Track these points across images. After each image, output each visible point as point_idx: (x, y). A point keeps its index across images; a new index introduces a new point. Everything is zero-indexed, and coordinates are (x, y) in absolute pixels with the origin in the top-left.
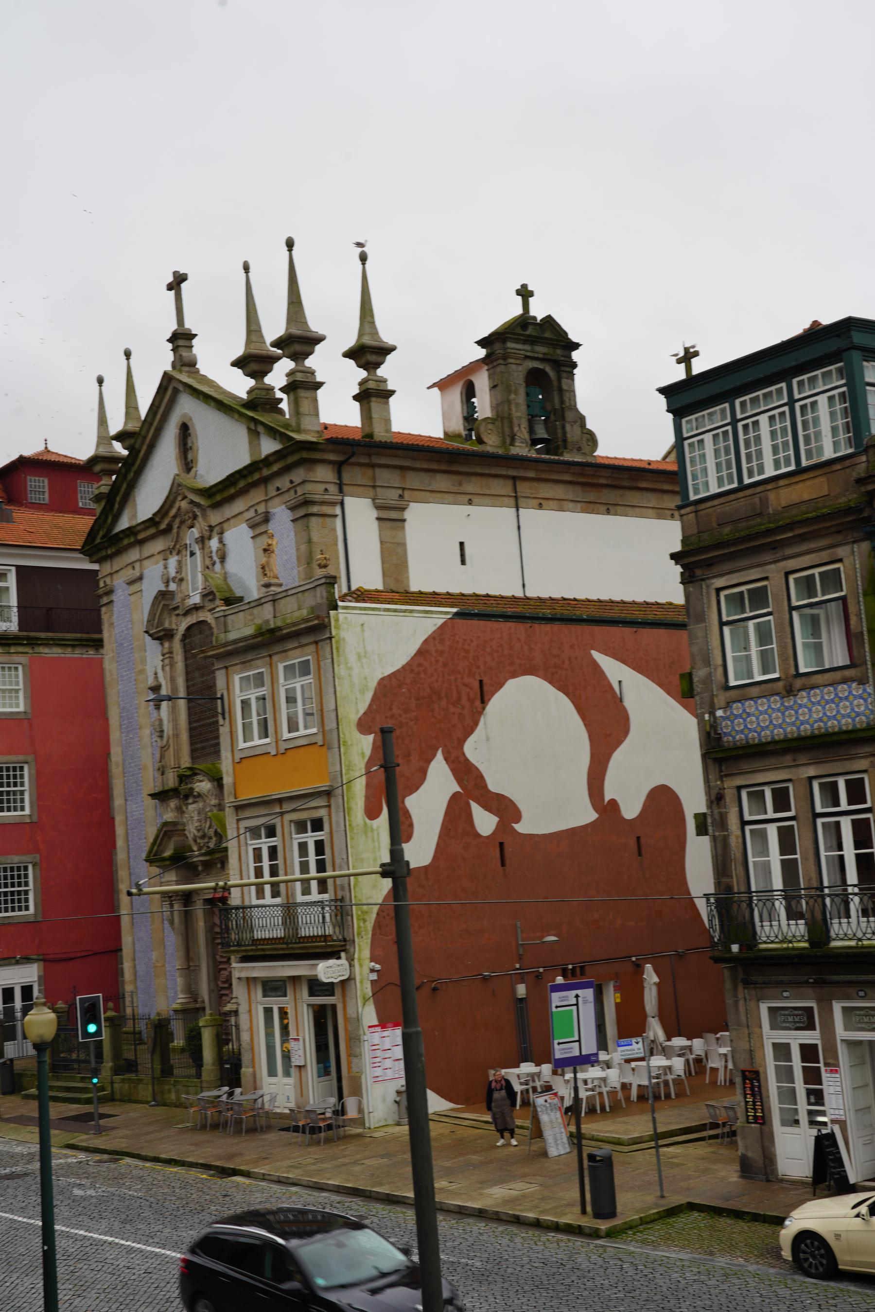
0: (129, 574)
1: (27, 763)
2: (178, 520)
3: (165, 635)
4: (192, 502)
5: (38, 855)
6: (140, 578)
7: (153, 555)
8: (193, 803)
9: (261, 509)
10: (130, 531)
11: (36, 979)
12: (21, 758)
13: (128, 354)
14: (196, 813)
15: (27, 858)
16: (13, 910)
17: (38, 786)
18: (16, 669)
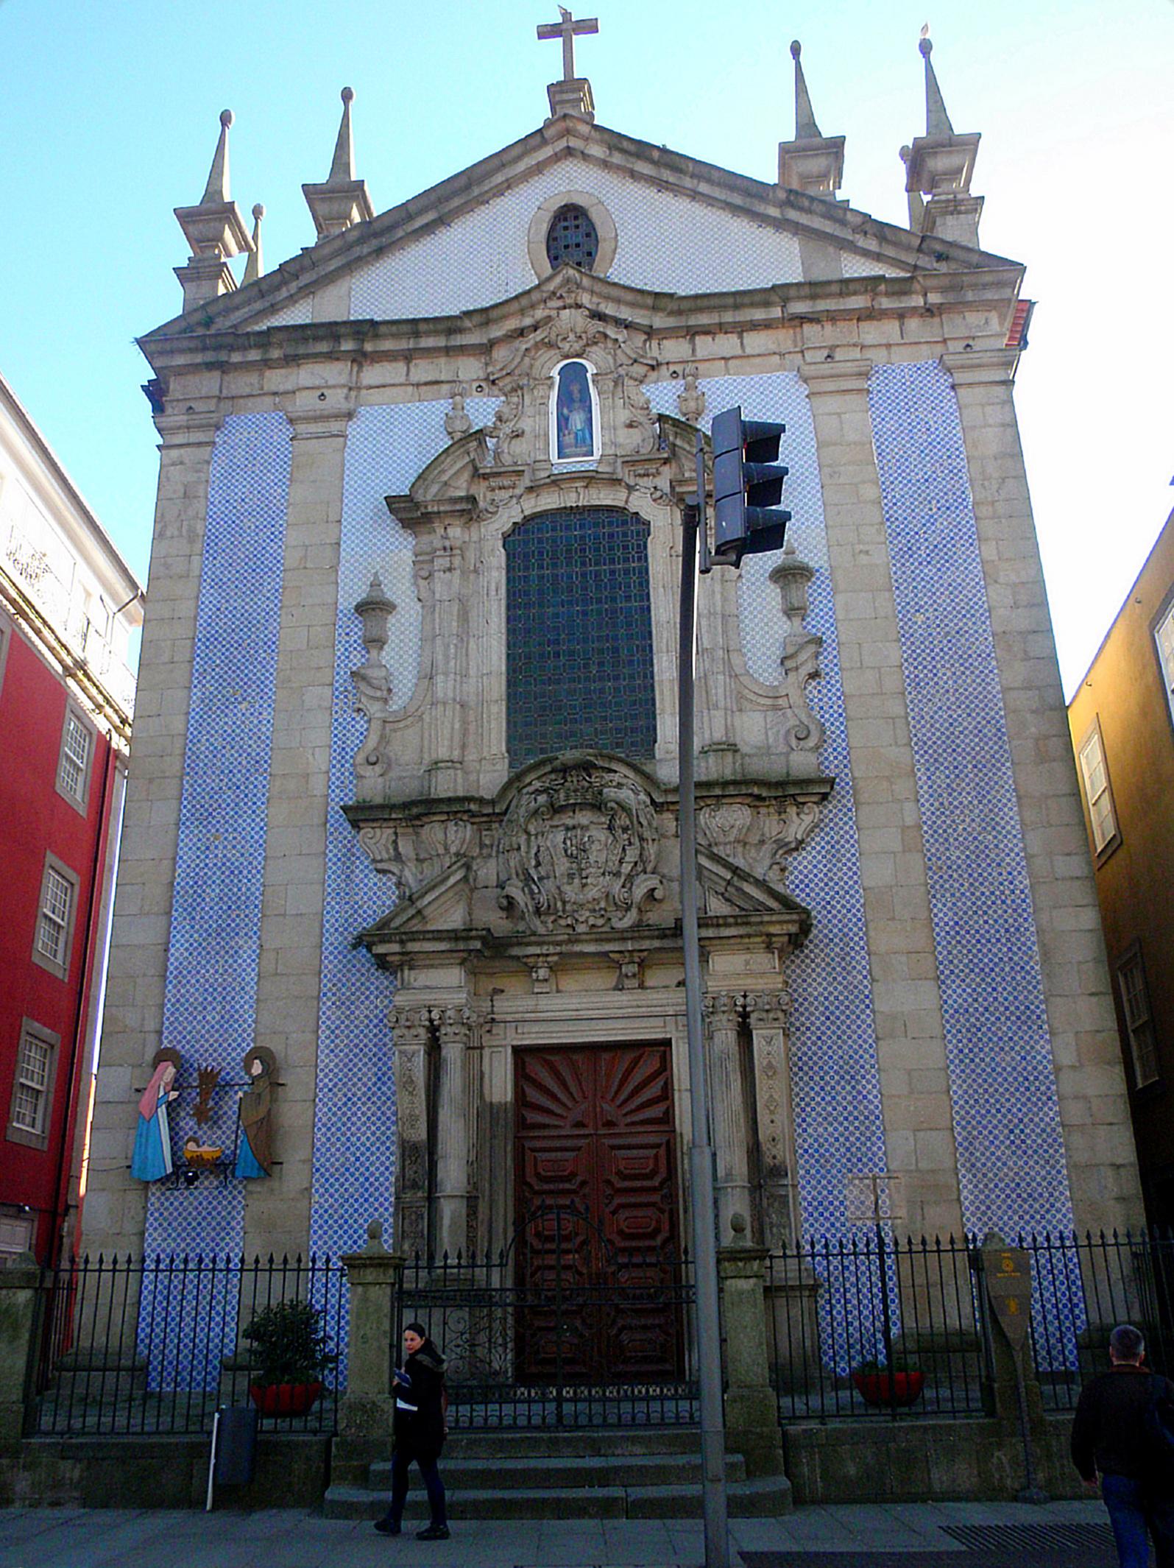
0: (306, 402)
4: (597, 316)
6: (350, 415)
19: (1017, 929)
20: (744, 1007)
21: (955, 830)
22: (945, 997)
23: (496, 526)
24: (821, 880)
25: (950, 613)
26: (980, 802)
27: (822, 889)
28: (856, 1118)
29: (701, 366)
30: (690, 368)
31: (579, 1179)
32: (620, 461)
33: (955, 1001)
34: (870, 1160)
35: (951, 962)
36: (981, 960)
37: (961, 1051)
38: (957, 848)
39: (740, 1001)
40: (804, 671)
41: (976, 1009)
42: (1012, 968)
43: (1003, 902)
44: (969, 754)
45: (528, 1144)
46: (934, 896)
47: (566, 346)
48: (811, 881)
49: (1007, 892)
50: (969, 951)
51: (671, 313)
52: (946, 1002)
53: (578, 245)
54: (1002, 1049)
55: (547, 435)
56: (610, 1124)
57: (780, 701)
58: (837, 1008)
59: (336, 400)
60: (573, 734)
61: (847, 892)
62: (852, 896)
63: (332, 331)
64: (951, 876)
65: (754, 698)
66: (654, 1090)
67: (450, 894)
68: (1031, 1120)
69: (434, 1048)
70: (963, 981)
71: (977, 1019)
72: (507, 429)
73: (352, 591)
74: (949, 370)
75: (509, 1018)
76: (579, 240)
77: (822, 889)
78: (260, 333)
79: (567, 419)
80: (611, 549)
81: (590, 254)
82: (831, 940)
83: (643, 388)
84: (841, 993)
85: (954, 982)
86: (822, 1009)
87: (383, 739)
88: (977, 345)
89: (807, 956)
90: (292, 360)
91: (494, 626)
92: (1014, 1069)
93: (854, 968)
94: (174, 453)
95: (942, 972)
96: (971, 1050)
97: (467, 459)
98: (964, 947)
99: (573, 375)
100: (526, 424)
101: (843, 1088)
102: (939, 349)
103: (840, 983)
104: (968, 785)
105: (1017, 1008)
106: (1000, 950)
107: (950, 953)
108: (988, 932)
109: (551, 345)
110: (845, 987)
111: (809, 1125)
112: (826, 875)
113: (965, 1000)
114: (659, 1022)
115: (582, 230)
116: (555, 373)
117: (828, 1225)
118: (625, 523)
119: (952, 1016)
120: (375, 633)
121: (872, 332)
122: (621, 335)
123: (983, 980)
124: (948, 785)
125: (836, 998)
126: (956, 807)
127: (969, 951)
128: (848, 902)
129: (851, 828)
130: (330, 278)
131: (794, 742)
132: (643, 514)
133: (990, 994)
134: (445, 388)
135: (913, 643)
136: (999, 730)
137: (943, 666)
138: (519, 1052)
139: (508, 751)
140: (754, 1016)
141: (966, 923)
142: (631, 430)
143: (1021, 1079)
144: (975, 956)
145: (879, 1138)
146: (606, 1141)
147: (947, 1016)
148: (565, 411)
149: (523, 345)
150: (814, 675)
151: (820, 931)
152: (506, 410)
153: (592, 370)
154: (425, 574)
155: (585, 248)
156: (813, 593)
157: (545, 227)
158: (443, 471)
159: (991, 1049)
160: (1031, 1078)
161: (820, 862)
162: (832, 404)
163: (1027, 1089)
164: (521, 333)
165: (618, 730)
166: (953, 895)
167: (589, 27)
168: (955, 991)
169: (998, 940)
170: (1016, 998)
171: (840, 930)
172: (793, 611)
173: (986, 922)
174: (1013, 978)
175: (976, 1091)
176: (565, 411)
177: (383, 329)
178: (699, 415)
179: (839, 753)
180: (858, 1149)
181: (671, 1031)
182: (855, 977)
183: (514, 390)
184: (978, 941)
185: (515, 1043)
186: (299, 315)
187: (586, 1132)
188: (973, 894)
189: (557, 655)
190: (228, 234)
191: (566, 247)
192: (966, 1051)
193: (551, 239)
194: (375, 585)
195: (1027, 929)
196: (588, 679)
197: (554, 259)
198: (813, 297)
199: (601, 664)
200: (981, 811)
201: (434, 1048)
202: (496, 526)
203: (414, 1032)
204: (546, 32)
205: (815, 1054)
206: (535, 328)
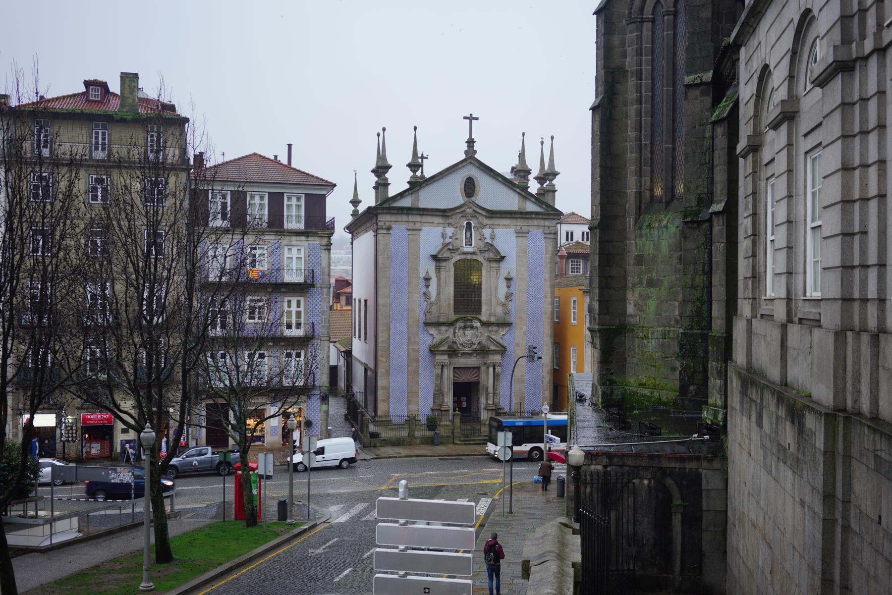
0: (411, 226)
4: (474, 210)
6: (420, 230)
9: (525, 228)
13: (415, 128)
30: (493, 227)
59: (418, 226)
63: (419, 209)
72: (454, 238)
74: (545, 234)
90: (408, 214)
99: (469, 224)
100: (458, 236)
116: (465, 224)
138: (454, 368)
153: (473, 225)
156: (513, 283)
172: (509, 287)
193: (465, 185)
204: (465, 118)
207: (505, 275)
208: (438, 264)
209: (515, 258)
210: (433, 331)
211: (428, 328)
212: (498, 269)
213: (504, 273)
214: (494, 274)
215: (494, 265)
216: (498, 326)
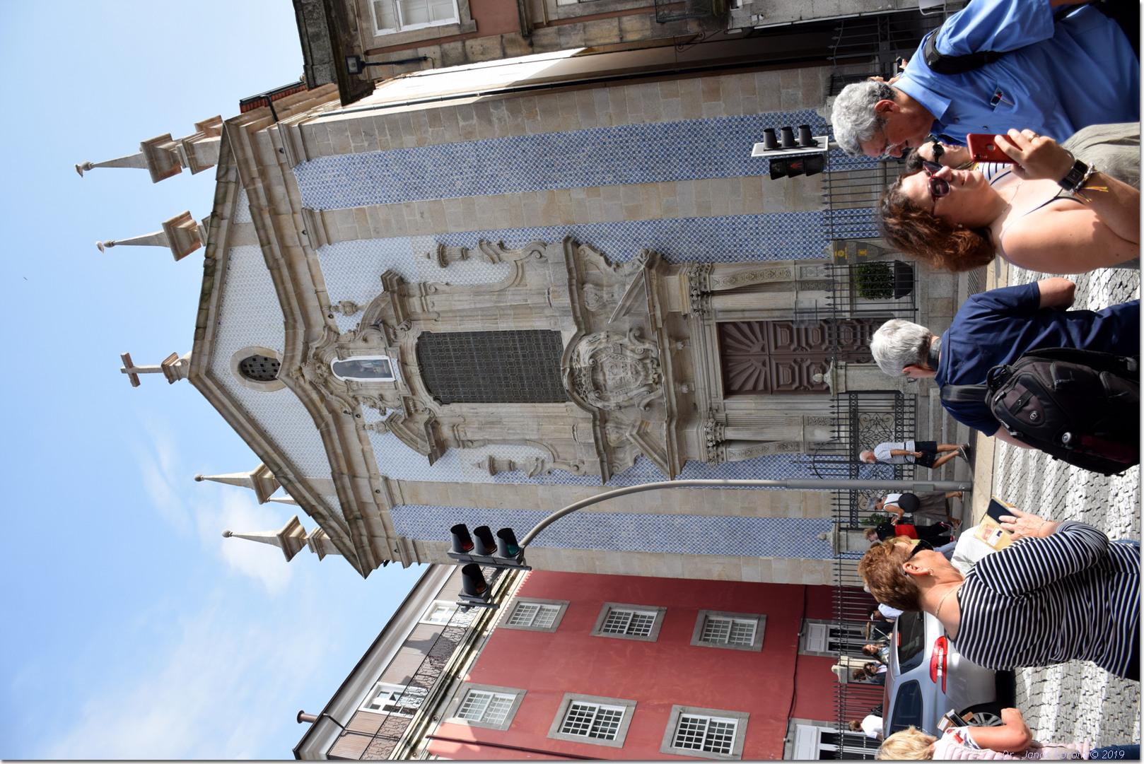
0: (383, 498)
1: (571, 701)
2: (324, 391)
3: (433, 428)
4: (304, 359)
5: (674, 706)
6: (386, 479)
7: (363, 450)
8: (604, 374)
10: (336, 476)
11: (816, 728)
12: (564, 705)
14: (615, 371)
15: (674, 715)
16: (730, 739)
17: (600, 694)
18: (473, 695)
19: (643, 134)
20: (698, 296)
21: (586, 168)
22: (685, 177)
23: (437, 409)
24: (622, 243)
25: (452, 166)
26: (567, 153)
27: (627, 243)
28: (757, 228)
29: (324, 302)
31: (793, 364)
32: (389, 348)
33: (688, 171)
34: (780, 221)
35: (665, 173)
36: (663, 156)
37: (717, 169)
38: (596, 167)
39: (695, 298)
40: (499, 251)
41: (692, 160)
42: (666, 138)
43: (627, 142)
44: (538, 158)
45: (775, 387)
46: (627, 181)
47: (326, 375)
48: (623, 249)
49: (621, 139)
50: (657, 162)
51: (295, 321)
52: (688, 177)
53: (262, 365)
54: (714, 146)
55: (381, 383)
56: (763, 349)
57: (519, 264)
58: (695, 237)
59: (379, 484)
60: (550, 370)
61: (628, 230)
62: (630, 227)
63: (340, 491)
64: (614, 171)
65: (519, 279)
66: (746, 329)
67: (646, 438)
68: (755, 131)
69: (729, 442)
70: (675, 167)
71: (698, 159)
72: (379, 403)
73: (484, 477)
74: (298, 162)
75: (709, 401)
76: (259, 364)
77: (627, 243)
78: (350, 524)
79: (366, 369)
80: (441, 351)
81: (266, 359)
82: (656, 239)
83: (342, 333)
84: (686, 234)
85: (676, 172)
86: (696, 245)
87: (565, 462)
88: (280, 146)
89: (666, 252)
91: (494, 410)
92: (726, 140)
93: (671, 227)
94: (421, 557)
95: (671, 178)
96: (716, 164)
97: (401, 426)
98: (655, 165)
100: (375, 394)
101: (740, 235)
102: (286, 167)
103: (681, 235)
104: (557, 159)
105: (690, 136)
106: (656, 145)
107: (659, 174)
108: (645, 151)
109: (326, 381)
110: (683, 232)
111: (761, 253)
112: (618, 241)
113: (687, 166)
114: (707, 328)
115: (252, 363)
116: (343, 379)
117: (816, 245)
118: (424, 344)
119: (696, 173)
120: (506, 467)
121: (284, 207)
122: (315, 345)
123: (674, 155)
124: (559, 171)
125: (689, 237)
126: (572, 166)
127: (657, 162)
128: (633, 229)
129: (590, 226)
130: (310, 489)
131: (543, 259)
132: (419, 335)
133: (682, 152)
134: (362, 433)
135: (474, 188)
136: (522, 140)
137: (486, 171)
139: (564, 402)
140: (703, 289)
141: (641, 163)
142: (368, 339)
143: (732, 136)
144: (660, 159)
145: (768, 216)
146: (773, 349)
147: (697, 176)
148: (362, 370)
149: (331, 398)
150: (501, 245)
151: (652, 245)
152: (369, 403)
153: (335, 360)
154: (470, 444)
155: (263, 362)
157: (255, 383)
158: (412, 439)
159: (715, 152)
160: (731, 130)
161: (611, 244)
162: (331, 231)
163: (737, 132)
164: (323, 398)
165: (546, 348)
166: (625, 171)
167: (127, 359)
168: (682, 172)
169: (650, 145)
170: (684, 137)
171: (650, 234)
172: (465, 254)
173: (640, 152)
174: (672, 138)
175: (739, 162)
176: (362, 370)
177: (335, 465)
178: (353, 304)
179: (546, 231)
180: (774, 227)
181: (713, 322)
182: (677, 227)
183: (355, 398)
184: (651, 157)
185: (722, 398)
186: (334, 502)
187: (768, 360)
188: (623, 159)
189: (506, 378)
190: (294, 534)
191: (264, 371)
192: (716, 166)
194: (479, 466)
195: (642, 128)
196: (518, 363)
197: (272, 378)
198: (269, 243)
199: (509, 356)
200: (573, 152)
201: (729, 442)
202: (437, 409)
203: (720, 453)
204: (136, 382)
205: (721, 249)
206: (319, 392)
207: (435, 262)
208: (452, 443)
209: (385, 243)
210: (626, 458)
211: (620, 470)
212: (425, 288)
213: (432, 272)
214: (438, 303)
215: (415, 303)
216: (582, 283)
